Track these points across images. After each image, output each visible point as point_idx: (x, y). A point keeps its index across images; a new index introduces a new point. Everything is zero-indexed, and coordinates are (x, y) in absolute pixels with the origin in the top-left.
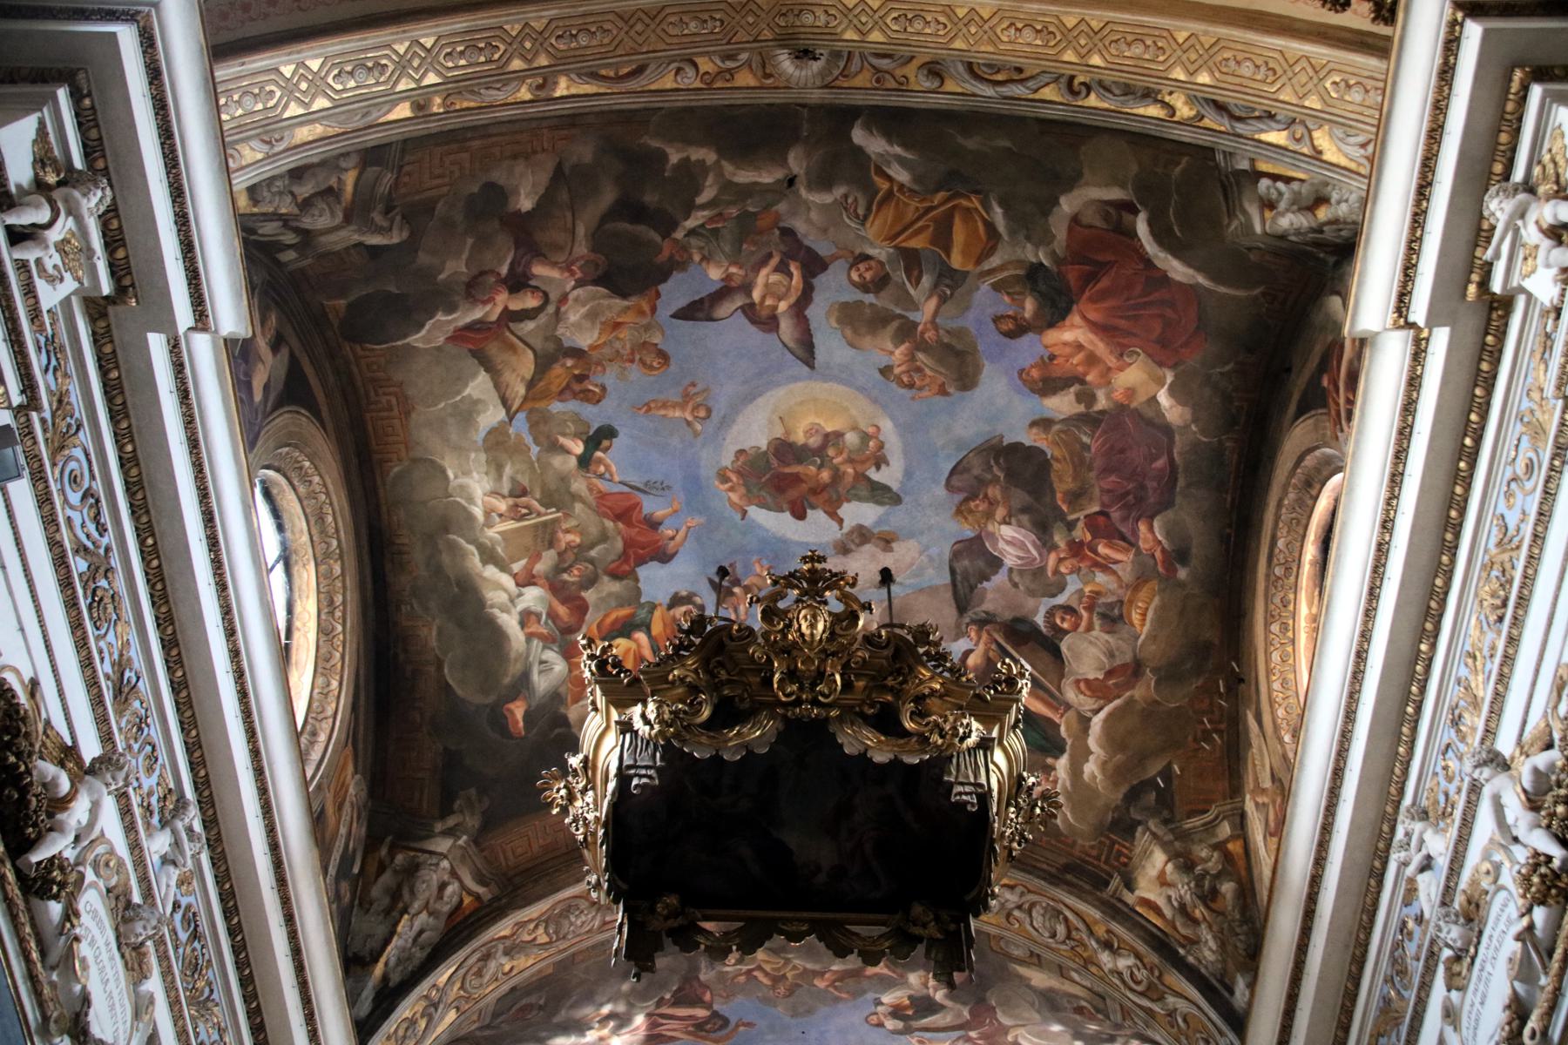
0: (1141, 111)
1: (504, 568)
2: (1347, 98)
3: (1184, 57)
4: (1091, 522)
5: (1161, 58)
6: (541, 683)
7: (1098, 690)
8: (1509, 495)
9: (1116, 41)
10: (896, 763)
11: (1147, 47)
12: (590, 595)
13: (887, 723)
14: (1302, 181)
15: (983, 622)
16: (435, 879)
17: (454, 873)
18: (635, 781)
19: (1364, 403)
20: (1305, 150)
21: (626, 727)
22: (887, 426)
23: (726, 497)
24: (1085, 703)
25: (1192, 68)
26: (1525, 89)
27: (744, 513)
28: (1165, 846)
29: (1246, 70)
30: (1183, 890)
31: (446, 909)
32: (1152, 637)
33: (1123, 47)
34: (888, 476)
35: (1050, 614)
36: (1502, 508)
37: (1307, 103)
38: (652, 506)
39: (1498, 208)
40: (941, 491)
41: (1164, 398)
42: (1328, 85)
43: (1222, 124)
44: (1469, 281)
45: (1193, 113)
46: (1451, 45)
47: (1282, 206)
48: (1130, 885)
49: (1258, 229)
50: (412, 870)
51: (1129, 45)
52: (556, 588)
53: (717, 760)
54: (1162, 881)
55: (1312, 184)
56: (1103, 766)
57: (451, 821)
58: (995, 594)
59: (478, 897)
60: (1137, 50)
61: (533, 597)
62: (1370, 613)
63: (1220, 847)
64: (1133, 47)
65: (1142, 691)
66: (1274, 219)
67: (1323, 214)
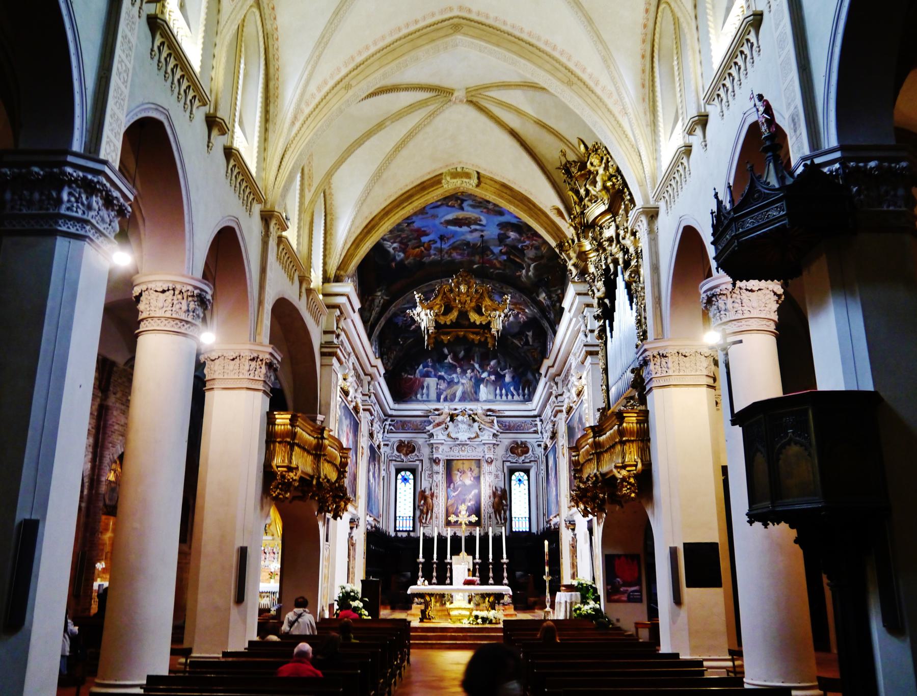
1: (388, 241)
4: (531, 234)
6: (398, 259)
7: (533, 260)
10: (481, 323)
12: (409, 243)
13: (480, 313)
15: (506, 245)
16: (378, 301)
17: (382, 298)
18: (430, 331)
21: (426, 315)
22: (482, 218)
23: (442, 228)
24: (530, 262)
27: (446, 227)
28: (545, 293)
30: (548, 303)
31: (381, 304)
32: (546, 252)
34: (484, 222)
35: (522, 246)
38: (423, 229)
40: (495, 226)
48: (538, 297)
50: (373, 300)
52: (400, 242)
53: (445, 323)
54: (544, 298)
56: (533, 274)
57: (380, 288)
58: (508, 241)
59: (387, 300)
61: (395, 245)
62: (567, 330)
63: (558, 295)
65: (544, 261)
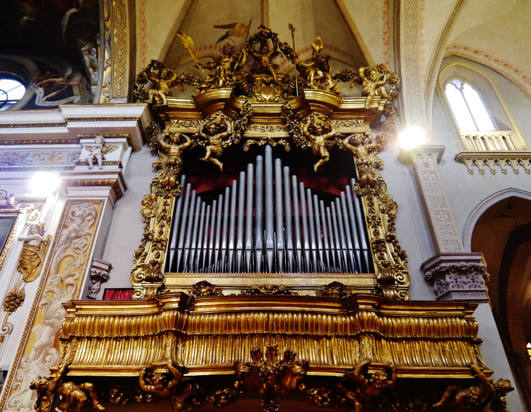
0: (105, 10)
2: (118, 84)
3: (120, 33)
5: (118, 25)
8: (35, 155)
9: (120, 10)
11: (120, 20)
14: (98, 62)
19: (44, 112)
20: (105, 65)
25: (117, 35)
26: (125, 137)
29: (120, 53)
33: (119, 12)
36: (31, 154)
37: (115, 72)
39: (99, 139)
41: (25, 18)
42: (120, 78)
43: (107, 38)
44: (81, 134)
45: (108, 27)
46: (131, 119)
47: (90, 56)
49: (83, 49)
51: (120, 14)
55: (98, 65)
60: (119, 17)
64: (119, 15)
66: (86, 54)
67: (91, 70)
